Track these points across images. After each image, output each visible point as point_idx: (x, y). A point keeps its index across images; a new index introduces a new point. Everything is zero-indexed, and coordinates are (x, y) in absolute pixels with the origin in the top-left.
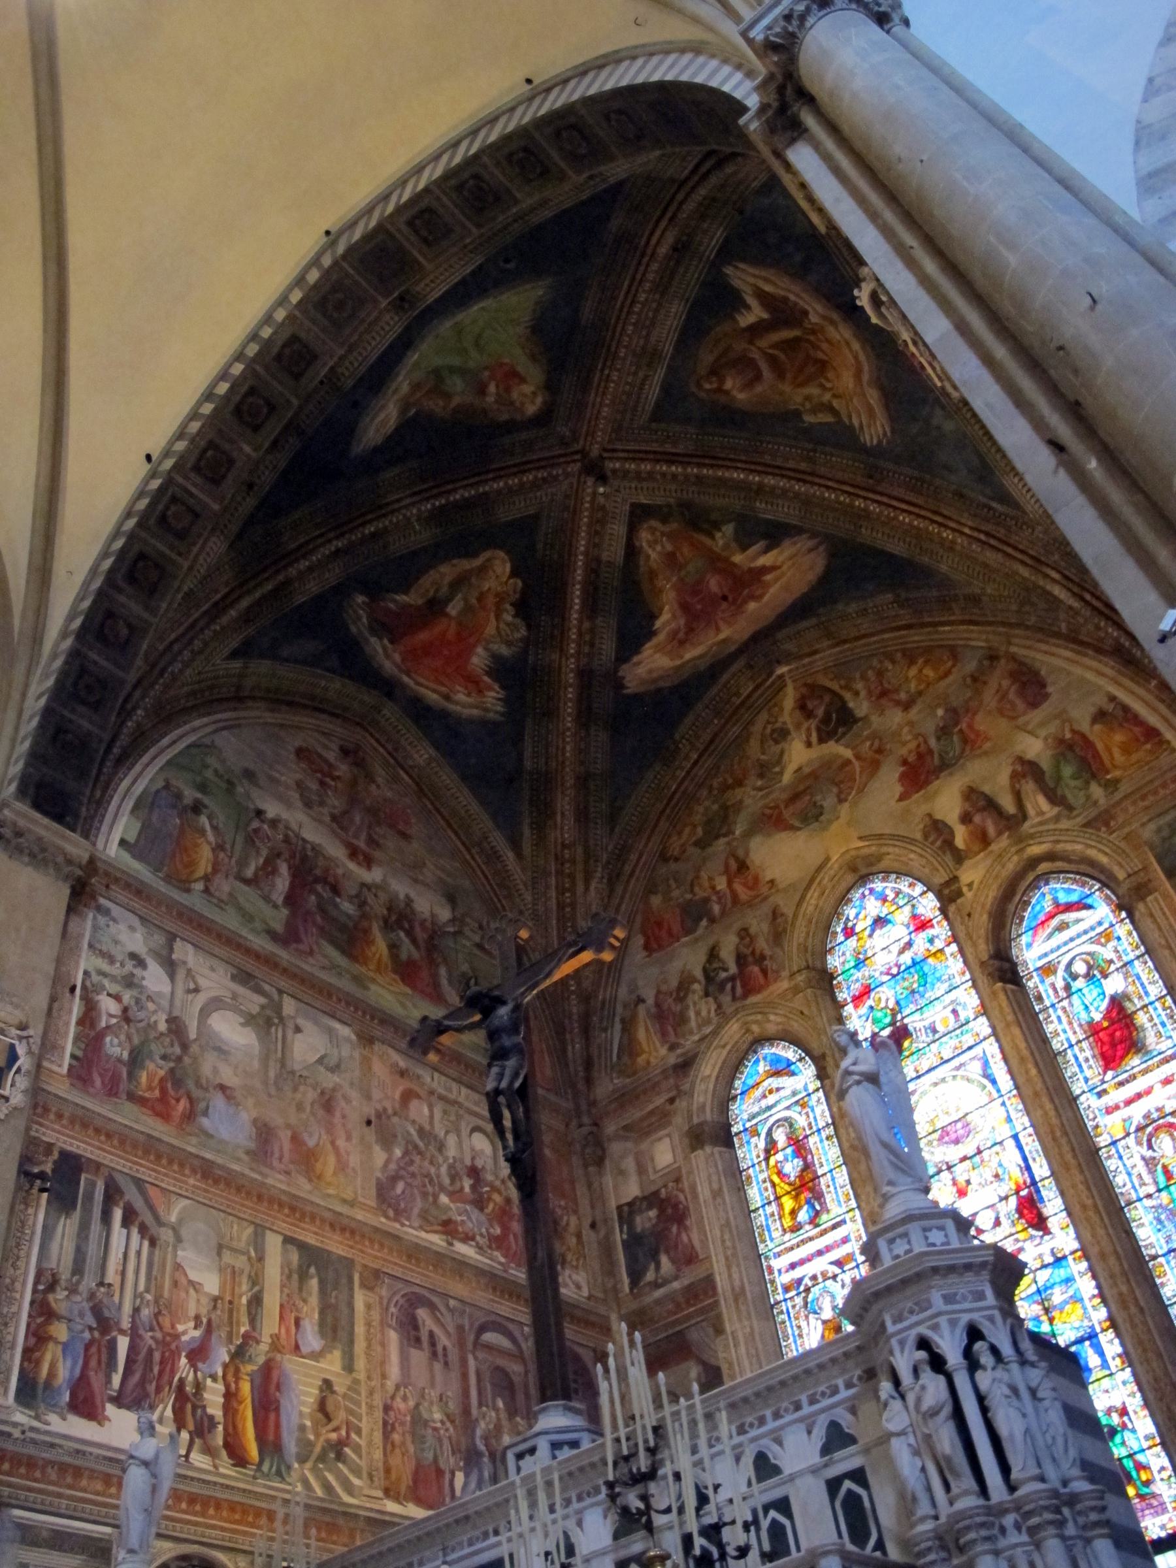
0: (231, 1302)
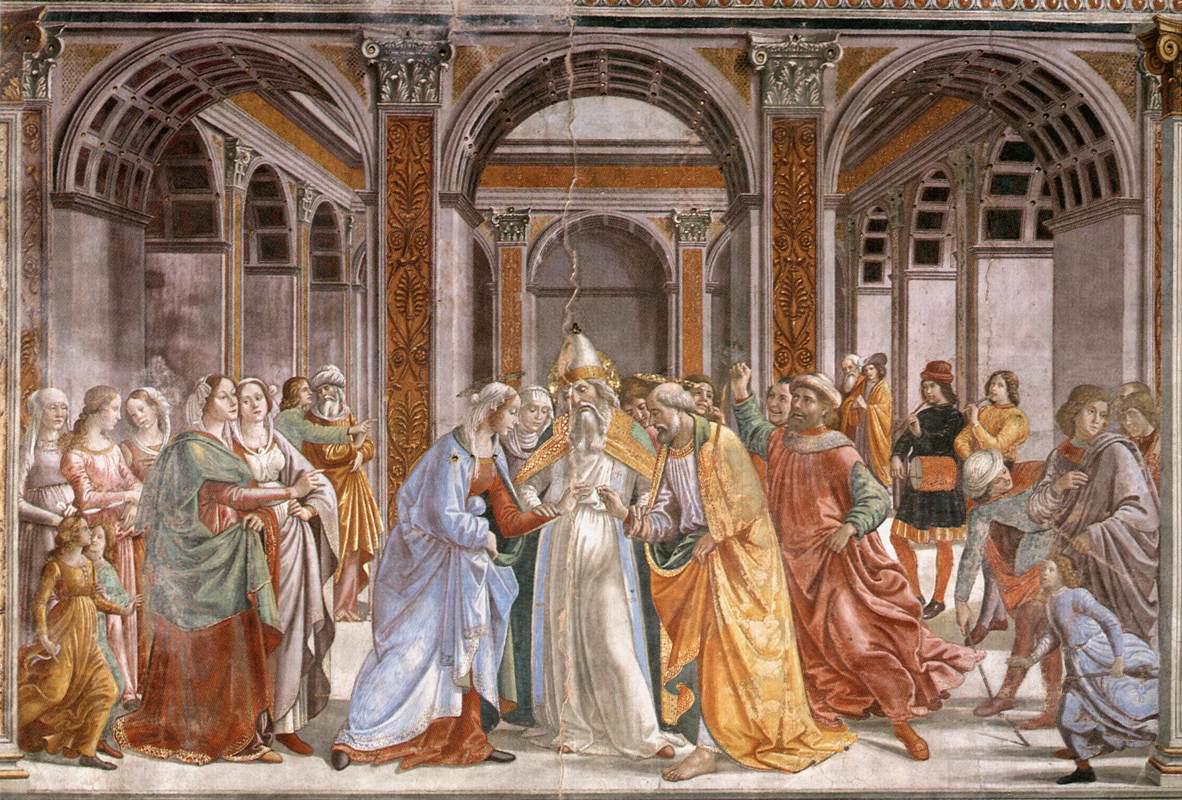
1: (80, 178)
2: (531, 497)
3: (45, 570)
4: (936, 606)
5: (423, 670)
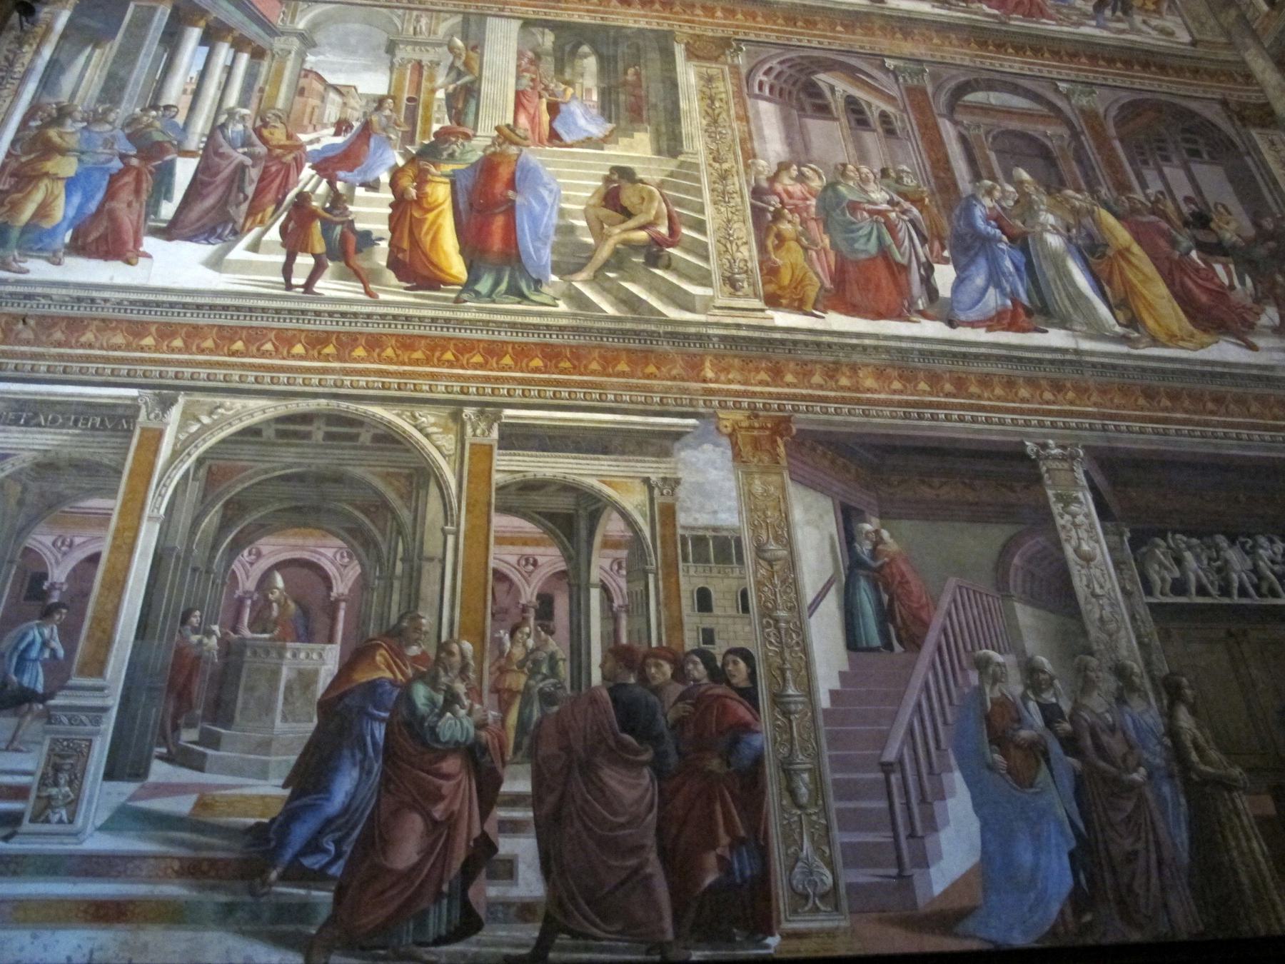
0: (409, 99)
1: (761, 88)
2: (1019, 223)
3: (768, 229)
4: (1232, 287)
5: (985, 290)
